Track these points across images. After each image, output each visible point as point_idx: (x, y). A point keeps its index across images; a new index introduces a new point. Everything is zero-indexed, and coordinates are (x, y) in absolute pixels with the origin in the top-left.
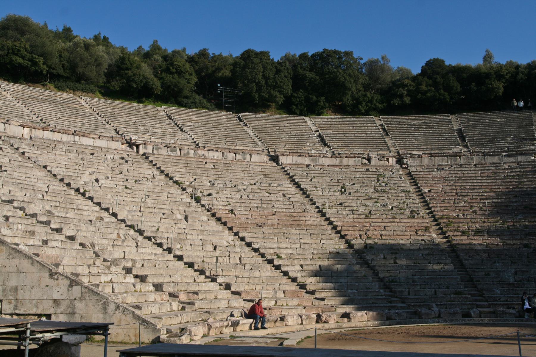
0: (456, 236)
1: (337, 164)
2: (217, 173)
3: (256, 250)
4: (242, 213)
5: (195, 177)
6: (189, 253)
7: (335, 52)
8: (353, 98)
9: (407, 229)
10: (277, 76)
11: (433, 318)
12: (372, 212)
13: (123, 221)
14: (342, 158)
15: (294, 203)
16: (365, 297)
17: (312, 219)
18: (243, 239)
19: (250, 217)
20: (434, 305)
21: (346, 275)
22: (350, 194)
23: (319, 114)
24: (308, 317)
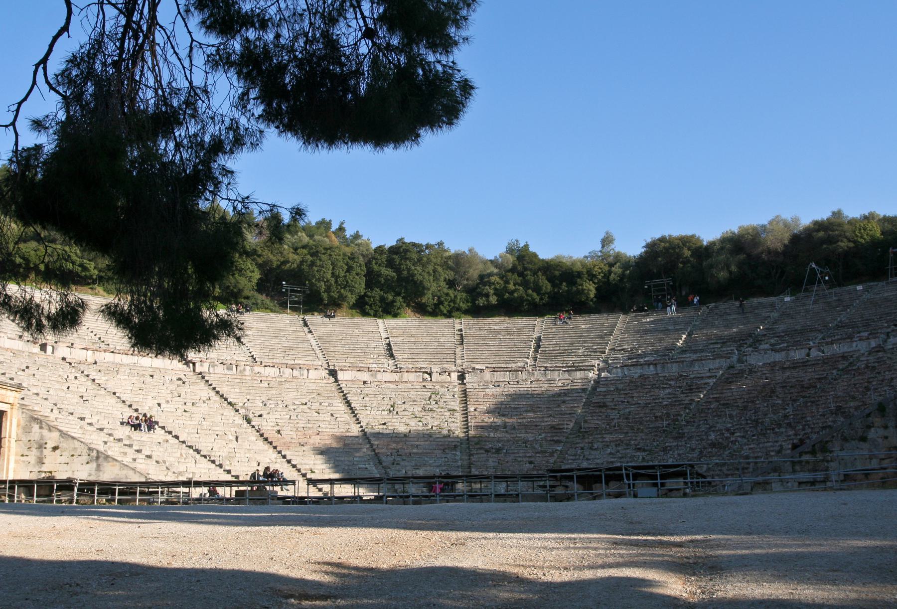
2: (271, 392)
3: (294, 466)
4: (287, 432)
5: (248, 398)
6: (236, 468)
7: (414, 245)
10: (348, 274)
13: (184, 442)
18: (284, 457)
19: (295, 437)
22: (397, 413)
23: (395, 315)
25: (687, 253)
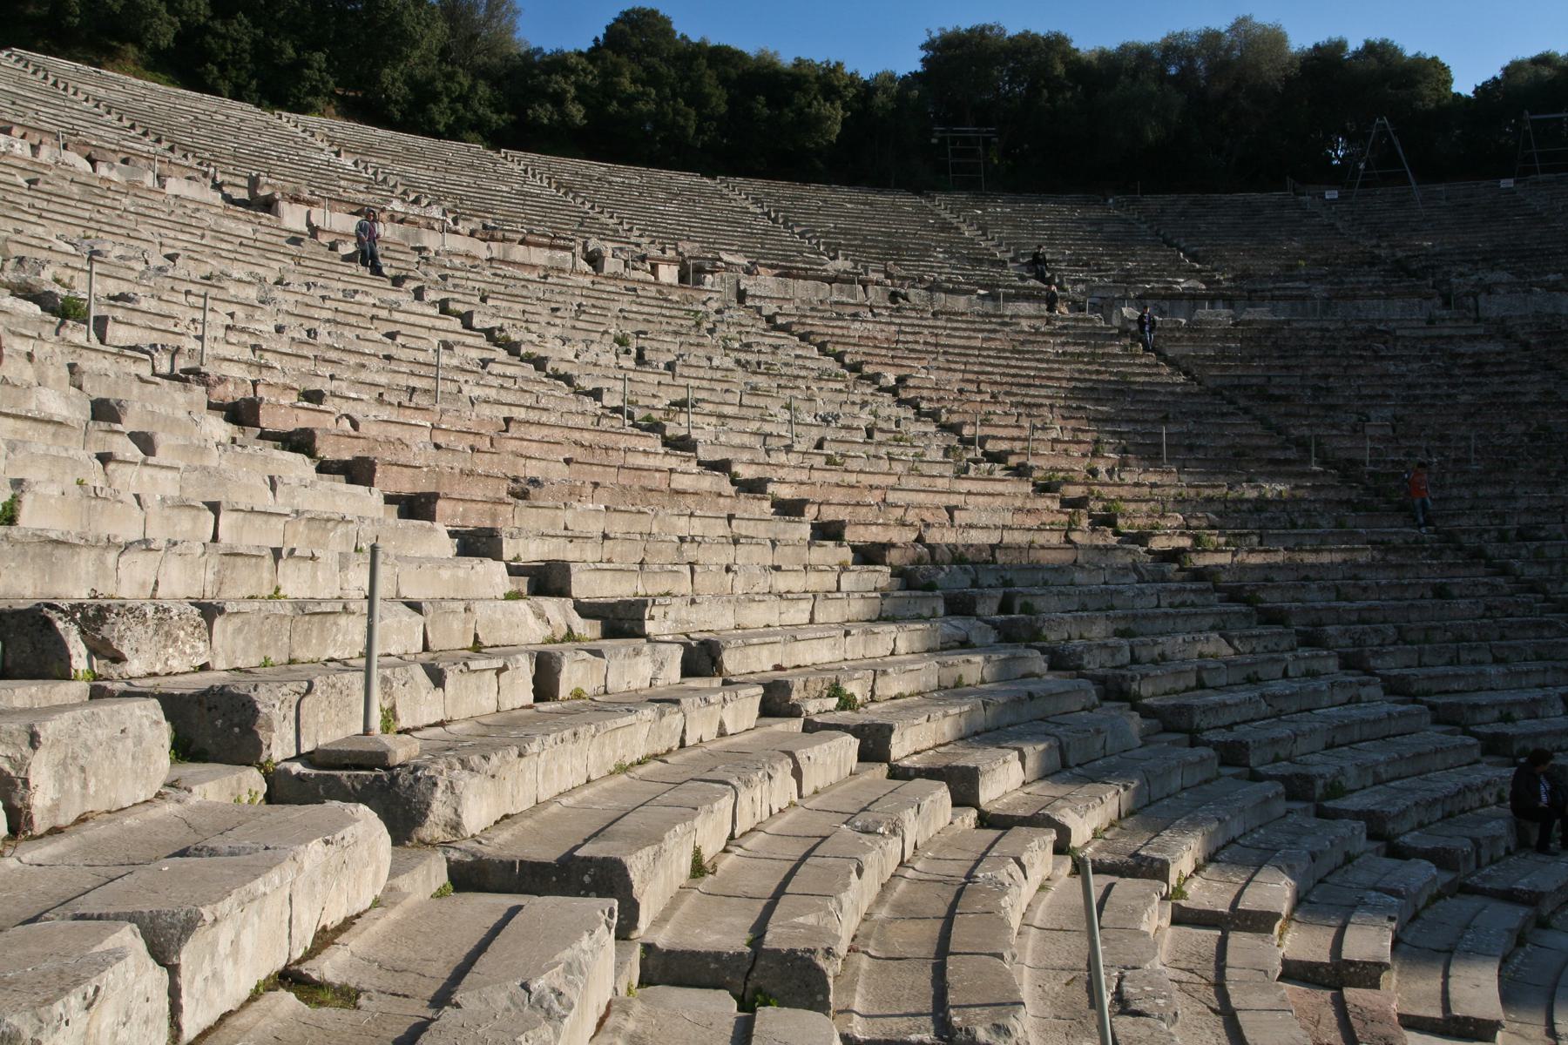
8: (411, 81)
12: (826, 445)
14: (507, 244)
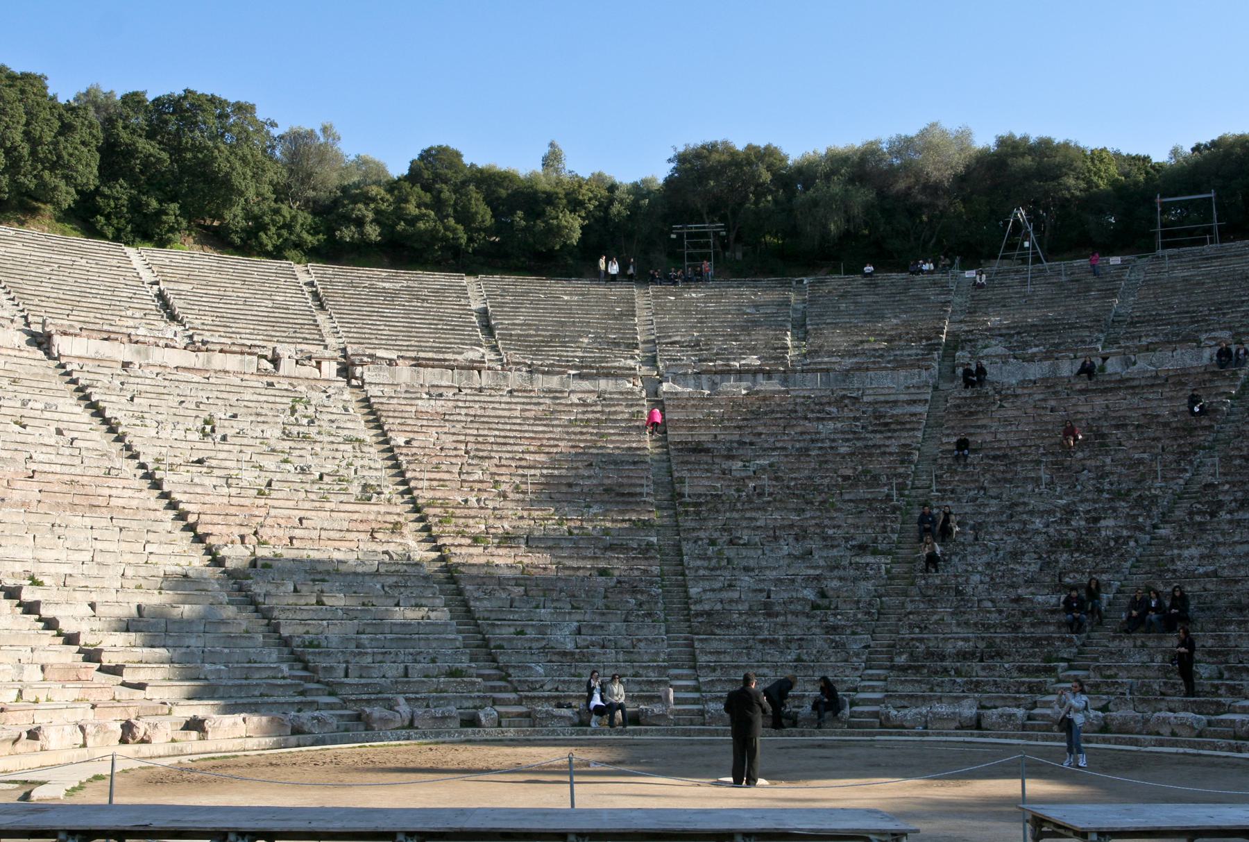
0: (460, 545)
1: (198, 366)
7: (212, 100)
8: (249, 215)
9: (353, 526)
10: (62, 139)
11: (397, 728)
12: (273, 483)
15: (84, 453)
16: (244, 682)
17: (129, 493)
20: (401, 699)
21: (202, 628)
22: (224, 438)
23: (162, 243)
24: (101, 728)
25: (766, 177)
